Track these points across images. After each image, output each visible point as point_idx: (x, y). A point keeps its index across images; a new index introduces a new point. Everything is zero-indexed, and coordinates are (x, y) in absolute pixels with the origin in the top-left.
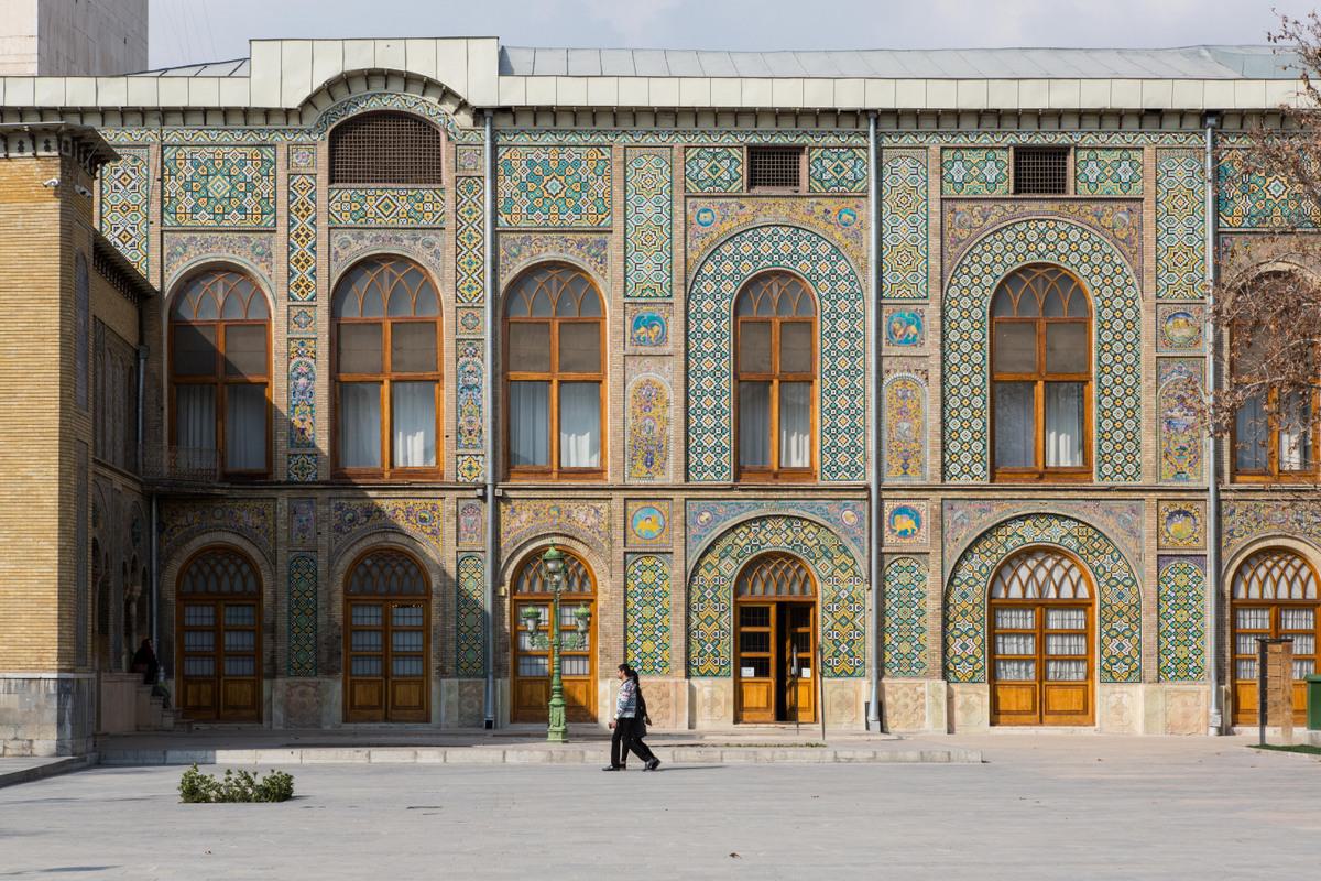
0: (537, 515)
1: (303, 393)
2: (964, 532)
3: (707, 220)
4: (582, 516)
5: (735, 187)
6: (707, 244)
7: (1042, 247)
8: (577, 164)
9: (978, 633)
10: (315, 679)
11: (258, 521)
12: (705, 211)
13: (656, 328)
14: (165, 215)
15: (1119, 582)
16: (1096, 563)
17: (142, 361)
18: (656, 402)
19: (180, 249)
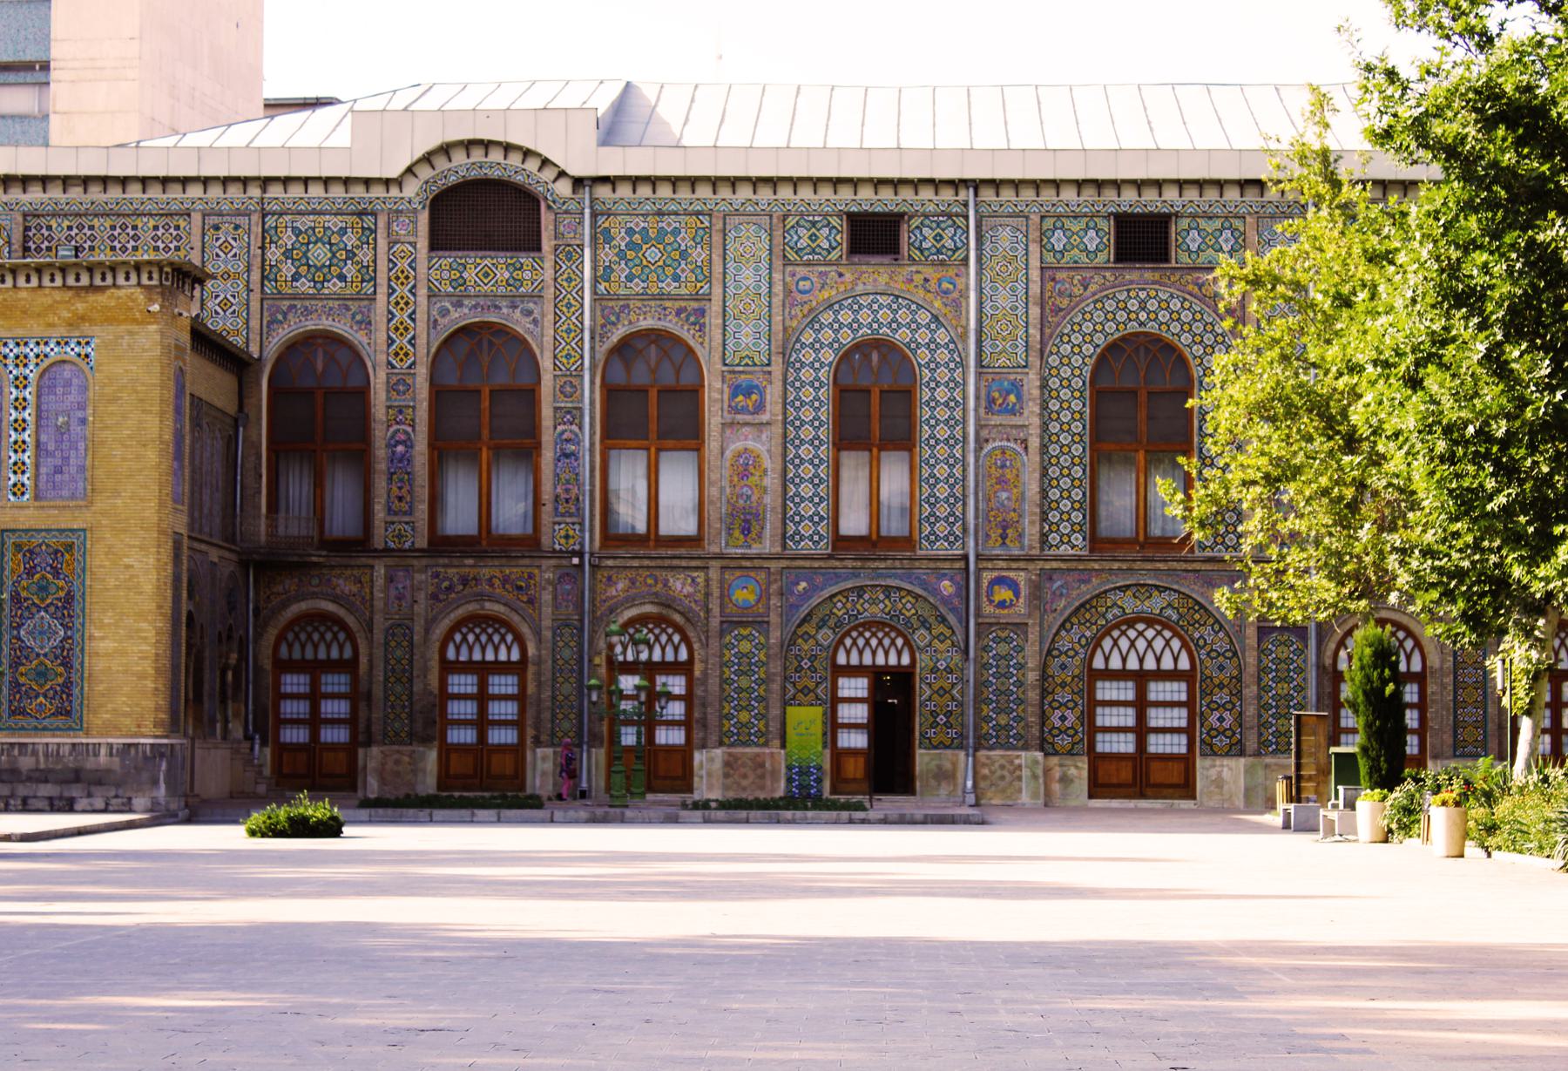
0: (633, 583)
1: (400, 461)
2: (1063, 603)
3: (807, 288)
4: (678, 585)
5: (834, 255)
6: (805, 312)
7: (1143, 316)
8: (676, 232)
9: (1076, 704)
10: (410, 748)
11: (355, 589)
12: (805, 279)
13: (754, 397)
14: (266, 283)
15: (1219, 654)
16: (1197, 635)
17: (241, 429)
18: (753, 471)
19: (280, 317)
